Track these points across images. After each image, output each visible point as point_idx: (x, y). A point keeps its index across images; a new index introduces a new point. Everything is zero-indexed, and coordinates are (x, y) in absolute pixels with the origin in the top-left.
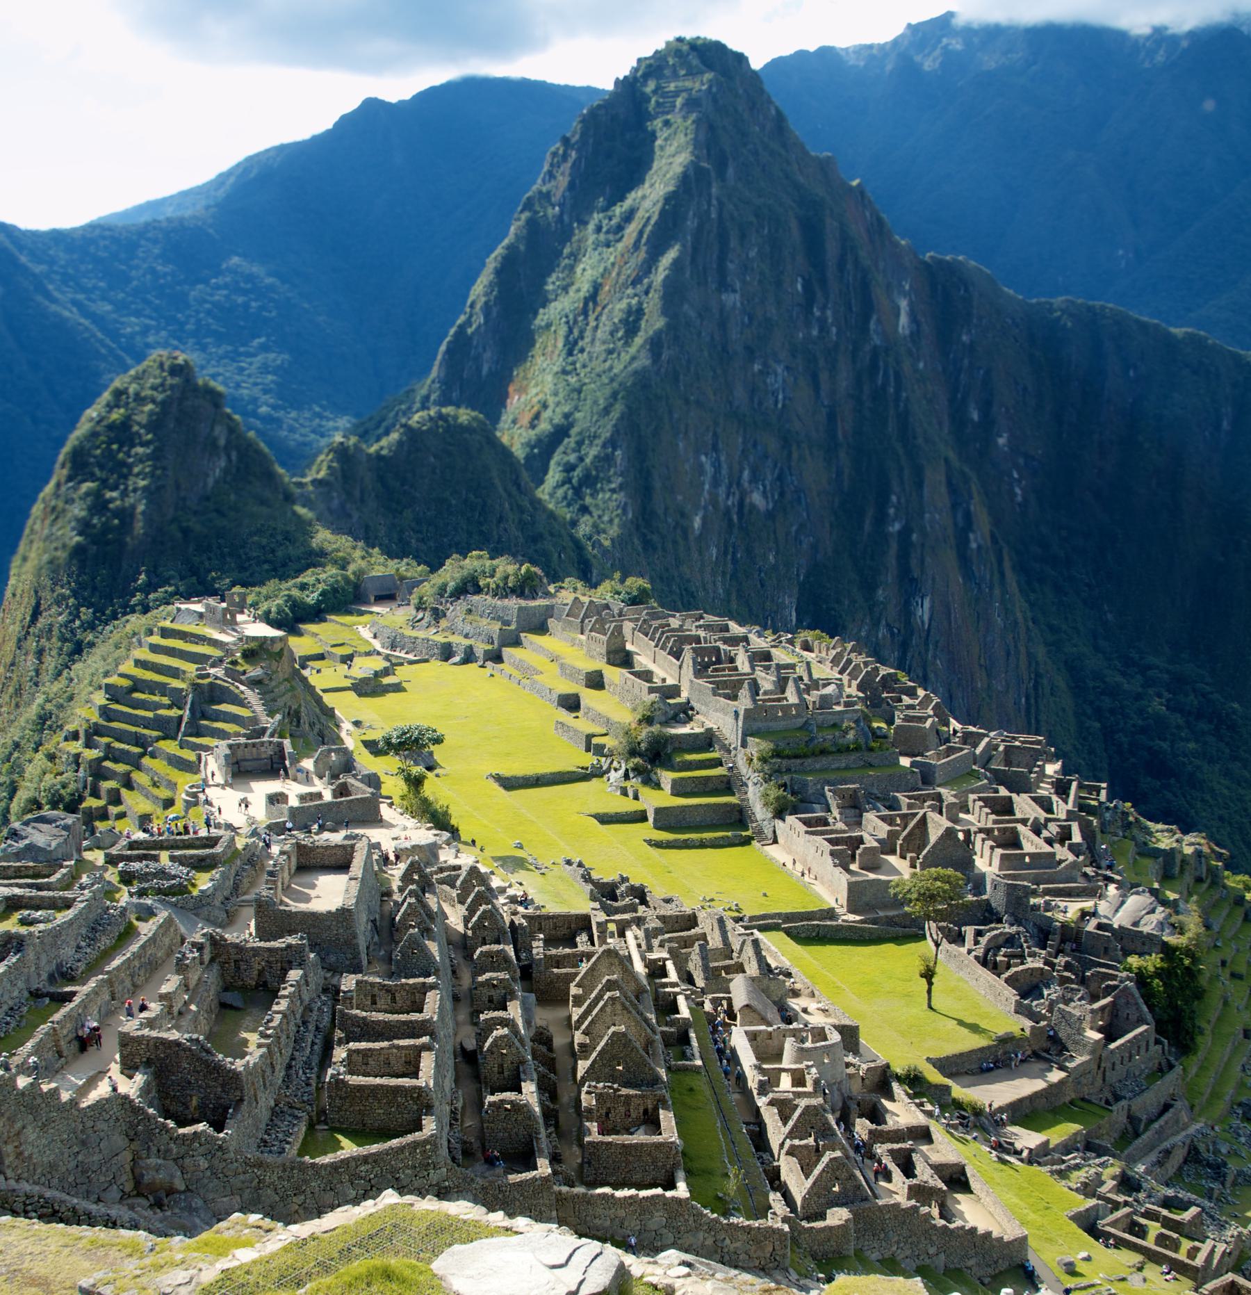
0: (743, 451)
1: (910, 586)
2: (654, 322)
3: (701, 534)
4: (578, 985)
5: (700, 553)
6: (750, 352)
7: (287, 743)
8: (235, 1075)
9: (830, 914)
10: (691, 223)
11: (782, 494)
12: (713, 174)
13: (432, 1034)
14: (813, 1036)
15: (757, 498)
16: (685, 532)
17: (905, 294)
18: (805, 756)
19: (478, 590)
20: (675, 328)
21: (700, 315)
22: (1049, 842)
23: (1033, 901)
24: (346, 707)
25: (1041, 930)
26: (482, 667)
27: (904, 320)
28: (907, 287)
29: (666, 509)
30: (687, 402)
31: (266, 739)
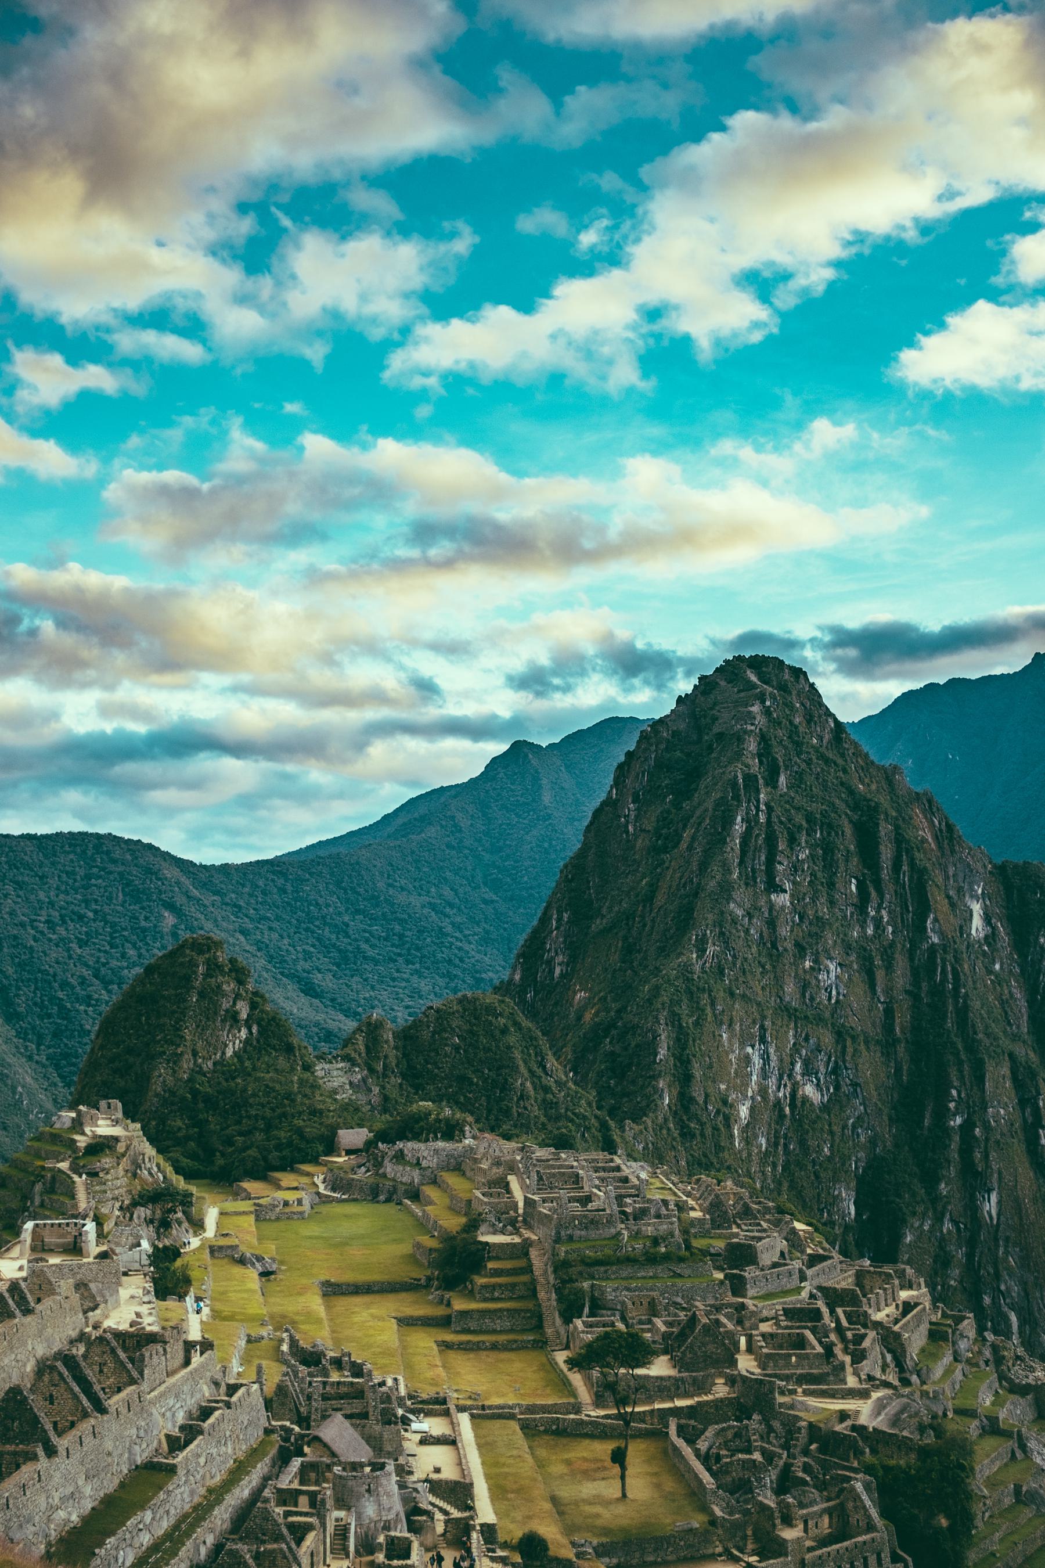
0: (794, 1044)
3: (747, 1125)
5: (747, 1141)
6: (801, 950)
10: (739, 826)
11: (837, 1088)
12: (761, 781)
16: (727, 1119)
17: (975, 897)
18: (613, 1264)
21: (750, 916)
23: (781, 1399)
27: (977, 922)
28: (980, 891)
29: (707, 1096)
30: (732, 994)
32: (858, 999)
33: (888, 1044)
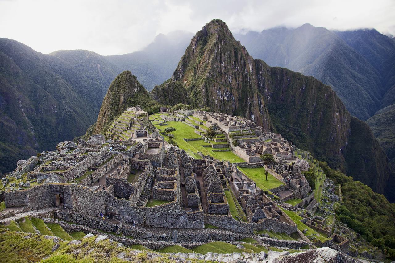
1: (251, 113)
2: (210, 67)
4: (205, 173)
7: (147, 131)
8: (132, 187)
9: (246, 163)
13: (176, 180)
14: (249, 184)
15: (226, 98)
19: (181, 109)
20: (213, 69)
21: (217, 68)
22: (285, 151)
24: (158, 127)
25: (285, 166)
26: (182, 122)
31: (143, 130)
32: (234, 81)
33: (238, 90)
